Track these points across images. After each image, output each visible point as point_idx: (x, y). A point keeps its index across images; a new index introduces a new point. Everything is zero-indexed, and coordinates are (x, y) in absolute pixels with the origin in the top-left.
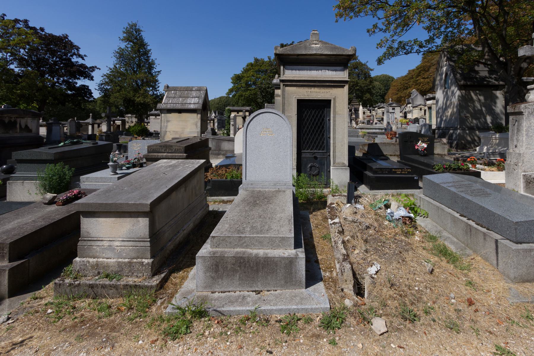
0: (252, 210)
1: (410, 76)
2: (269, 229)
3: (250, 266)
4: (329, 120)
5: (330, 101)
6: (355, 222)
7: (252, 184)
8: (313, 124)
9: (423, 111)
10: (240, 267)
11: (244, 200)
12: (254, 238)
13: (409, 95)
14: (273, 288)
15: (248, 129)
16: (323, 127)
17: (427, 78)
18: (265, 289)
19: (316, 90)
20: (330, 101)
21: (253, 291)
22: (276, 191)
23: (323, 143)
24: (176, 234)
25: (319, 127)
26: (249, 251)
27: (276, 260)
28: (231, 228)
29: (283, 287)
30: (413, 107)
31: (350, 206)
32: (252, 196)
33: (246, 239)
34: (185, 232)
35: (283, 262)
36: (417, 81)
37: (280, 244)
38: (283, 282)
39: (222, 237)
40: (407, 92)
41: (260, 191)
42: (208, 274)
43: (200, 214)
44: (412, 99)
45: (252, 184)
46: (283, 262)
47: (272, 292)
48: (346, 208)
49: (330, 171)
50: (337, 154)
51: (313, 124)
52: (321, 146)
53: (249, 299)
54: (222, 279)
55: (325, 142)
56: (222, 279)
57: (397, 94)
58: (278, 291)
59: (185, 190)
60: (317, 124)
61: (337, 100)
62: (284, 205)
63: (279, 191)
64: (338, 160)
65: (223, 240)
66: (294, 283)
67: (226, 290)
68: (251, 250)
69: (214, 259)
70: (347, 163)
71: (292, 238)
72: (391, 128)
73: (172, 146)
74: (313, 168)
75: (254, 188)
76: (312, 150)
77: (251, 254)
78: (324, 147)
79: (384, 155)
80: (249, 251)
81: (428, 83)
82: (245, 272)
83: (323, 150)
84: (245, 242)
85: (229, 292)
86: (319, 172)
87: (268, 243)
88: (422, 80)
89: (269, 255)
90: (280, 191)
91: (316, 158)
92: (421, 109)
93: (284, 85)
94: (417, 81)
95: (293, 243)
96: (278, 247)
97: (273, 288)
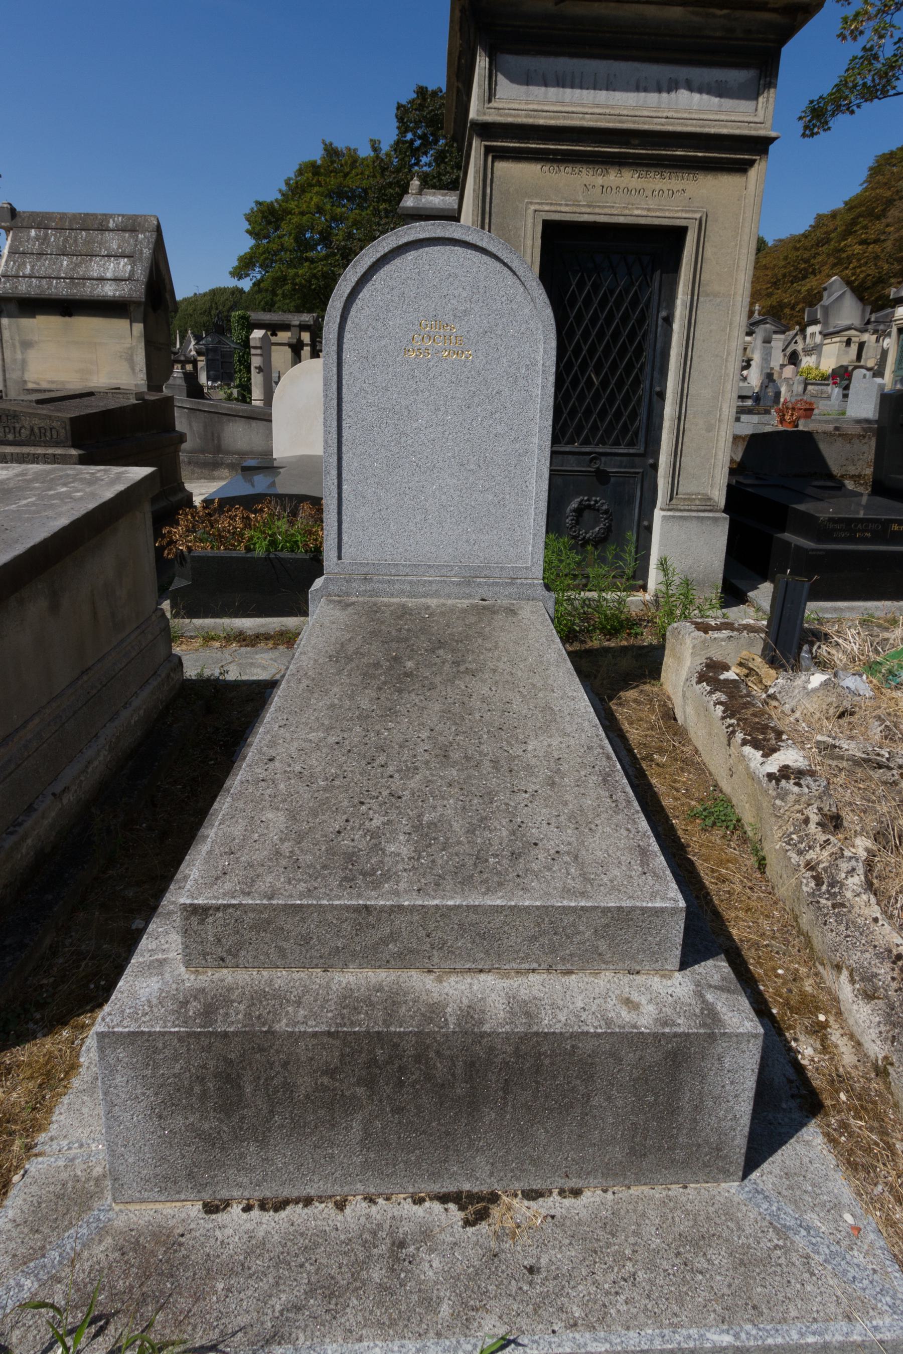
0: (391, 712)
1: (819, 234)
2: (521, 849)
3: (429, 1077)
4: (669, 321)
5: (682, 232)
6: (880, 766)
7: (366, 579)
8: (601, 335)
9: (854, 348)
10: (369, 1083)
11: (341, 656)
12: (445, 912)
13: (814, 298)
14: (561, 1182)
15: (349, 325)
16: (639, 350)
17: (876, 241)
18: (517, 1186)
19: (628, 178)
20: (682, 232)
21: (444, 1199)
22: (474, 607)
23: (634, 415)
24: (17, 824)
25: (623, 350)
26: (420, 983)
27: (588, 1046)
28: (300, 837)
29: (612, 1174)
30: (825, 335)
31: (825, 684)
32: (375, 634)
33: (400, 921)
34: (69, 798)
35: (630, 1057)
36: (842, 250)
37: (603, 946)
38: (618, 1153)
39: (254, 908)
40: (812, 283)
41: (403, 606)
42: (179, 1122)
43: (137, 707)
44: (826, 310)
45: (366, 579)
46: (630, 1057)
47: (554, 1204)
48: (809, 694)
49: (649, 529)
50: (688, 461)
51: (601, 335)
52: (625, 429)
53: (431, 1267)
54: (263, 1143)
55: (643, 410)
56: (263, 1143)
57: (769, 295)
58: (588, 1196)
59: (54, 608)
60: (616, 335)
61: (713, 230)
62: (537, 680)
63: (486, 611)
64: (687, 487)
65: (260, 926)
66: (679, 1154)
67: (286, 1192)
68: (429, 981)
69: (208, 1049)
70: (719, 496)
71: (674, 911)
72: (778, 394)
73: (15, 416)
74: (586, 514)
75: (373, 593)
76: (586, 442)
77: (435, 1010)
78: (636, 434)
79: (830, 476)
80: (420, 983)
81: (877, 257)
82: (398, 1110)
83: (631, 444)
84: (393, 937)
85: (308, 1201)
86: (609, 529)
87: (534, 938)
88: (858, 249)
89: (547, 1022)
90: (492, 611)
91: (602, 476)
92: (848, 342)
93: (488, 150)
94: (842, 250)
95: (679, 940)
96: (588, 960)
97: (561, 1182)
